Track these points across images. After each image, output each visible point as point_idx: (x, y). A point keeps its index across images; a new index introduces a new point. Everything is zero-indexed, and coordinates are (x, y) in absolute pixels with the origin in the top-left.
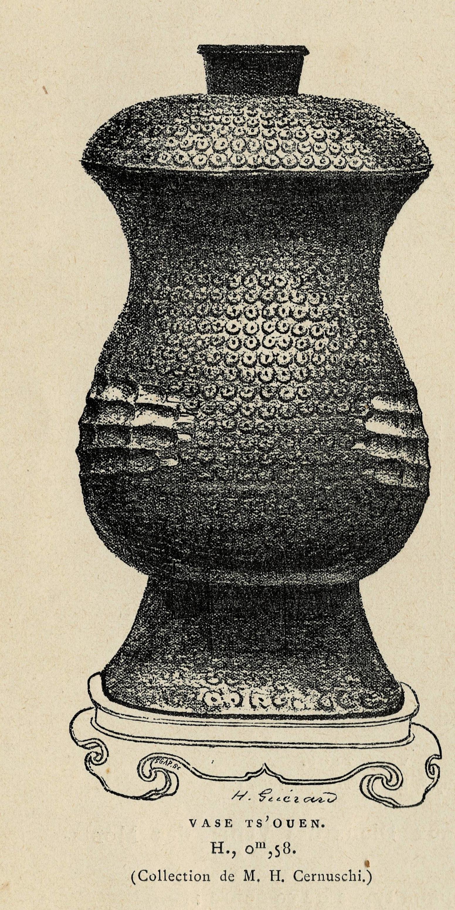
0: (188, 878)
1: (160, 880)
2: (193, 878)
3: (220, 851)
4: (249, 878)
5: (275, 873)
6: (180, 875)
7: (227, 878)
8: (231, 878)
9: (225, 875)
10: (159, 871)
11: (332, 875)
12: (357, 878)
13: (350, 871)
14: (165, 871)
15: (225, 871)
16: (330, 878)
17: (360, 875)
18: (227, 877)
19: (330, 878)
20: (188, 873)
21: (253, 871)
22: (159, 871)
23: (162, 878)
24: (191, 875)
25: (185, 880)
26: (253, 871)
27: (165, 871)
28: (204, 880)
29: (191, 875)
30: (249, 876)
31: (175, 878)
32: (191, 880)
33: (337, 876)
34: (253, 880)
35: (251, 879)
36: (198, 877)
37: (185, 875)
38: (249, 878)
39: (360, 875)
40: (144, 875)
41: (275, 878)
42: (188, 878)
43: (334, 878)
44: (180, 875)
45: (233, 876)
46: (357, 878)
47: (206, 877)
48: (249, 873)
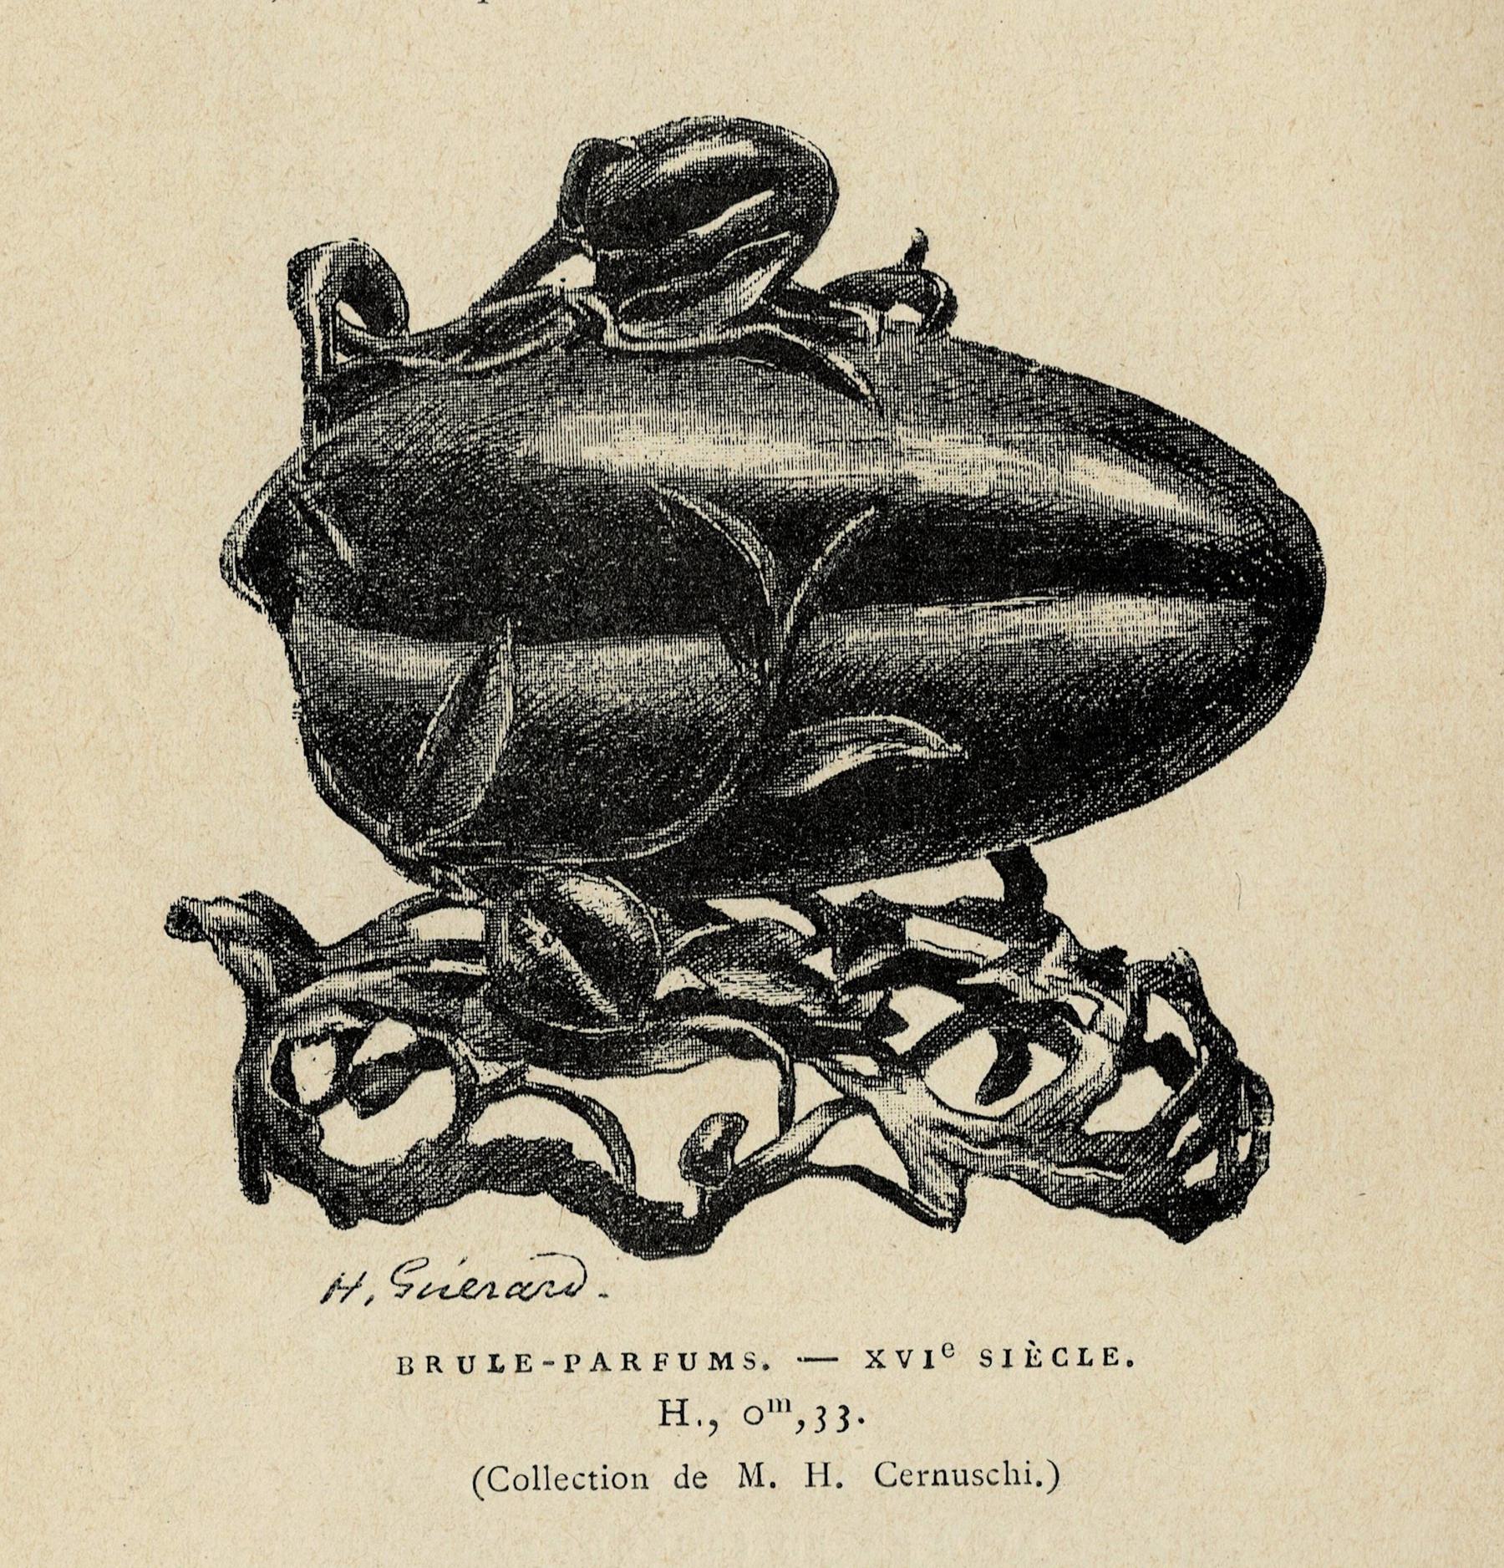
0: (598, 1482)
1: (536, 1488)
2: (609, 1484)
3: (679, 1421)
4: (750, 1481)
5: (818, 1468)
6: (582, 1475)
7: (690, 1483)
8: (700, 1482)
9: (686, 1475)
10: (535, 1467)
11: (965, 1471)
12: (1023, 1479)
13: (1006, 1462)
14: (546, 1467)
15: (686, 1466)
16: (961, 1479)
17: (1028, 1471)
18: (692, 1480)
19: (961, 1479)
20: (599, 1472)
21: (758, 1465)
22: (535, 1467)
23: (542, 1484)
24: (604, 1476)
25: (593, 1488)
26: (758, 1465)
27: (546, 1467)
28: (635, 1487)
29: (604, 1476)
30: (752, 1476)
31: (569, 1483)
32: (605, 1487)
33: (978, 1473)
34: (760, 1484)
35: (755, 1481)
36: (620, 1481)
37: (592, 1475)
38: (750, 1481)
39: (1028, 1471)
40: (500, 1479)
41: (818, 1480)
42: (598, 1482)
43: (970, 1478)
44: (582, 1475)
45: (704, 1477)
46: (1023, 1479)
47: (640, 1480)
48: (751, 1468)
